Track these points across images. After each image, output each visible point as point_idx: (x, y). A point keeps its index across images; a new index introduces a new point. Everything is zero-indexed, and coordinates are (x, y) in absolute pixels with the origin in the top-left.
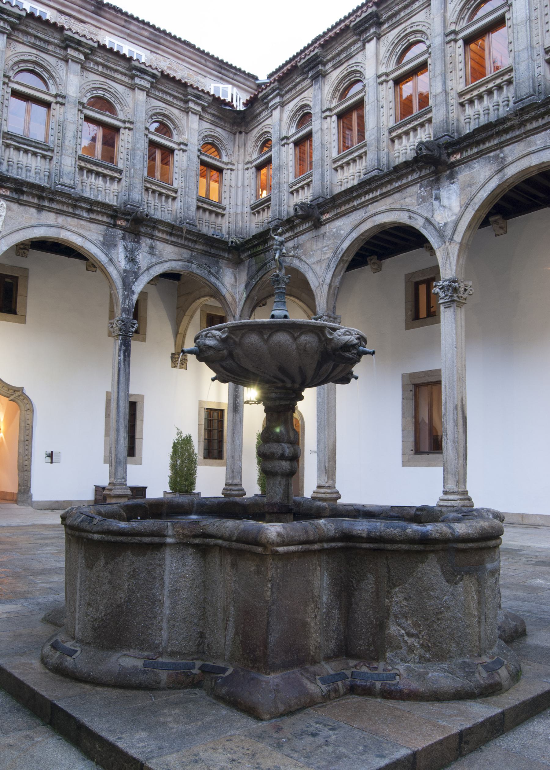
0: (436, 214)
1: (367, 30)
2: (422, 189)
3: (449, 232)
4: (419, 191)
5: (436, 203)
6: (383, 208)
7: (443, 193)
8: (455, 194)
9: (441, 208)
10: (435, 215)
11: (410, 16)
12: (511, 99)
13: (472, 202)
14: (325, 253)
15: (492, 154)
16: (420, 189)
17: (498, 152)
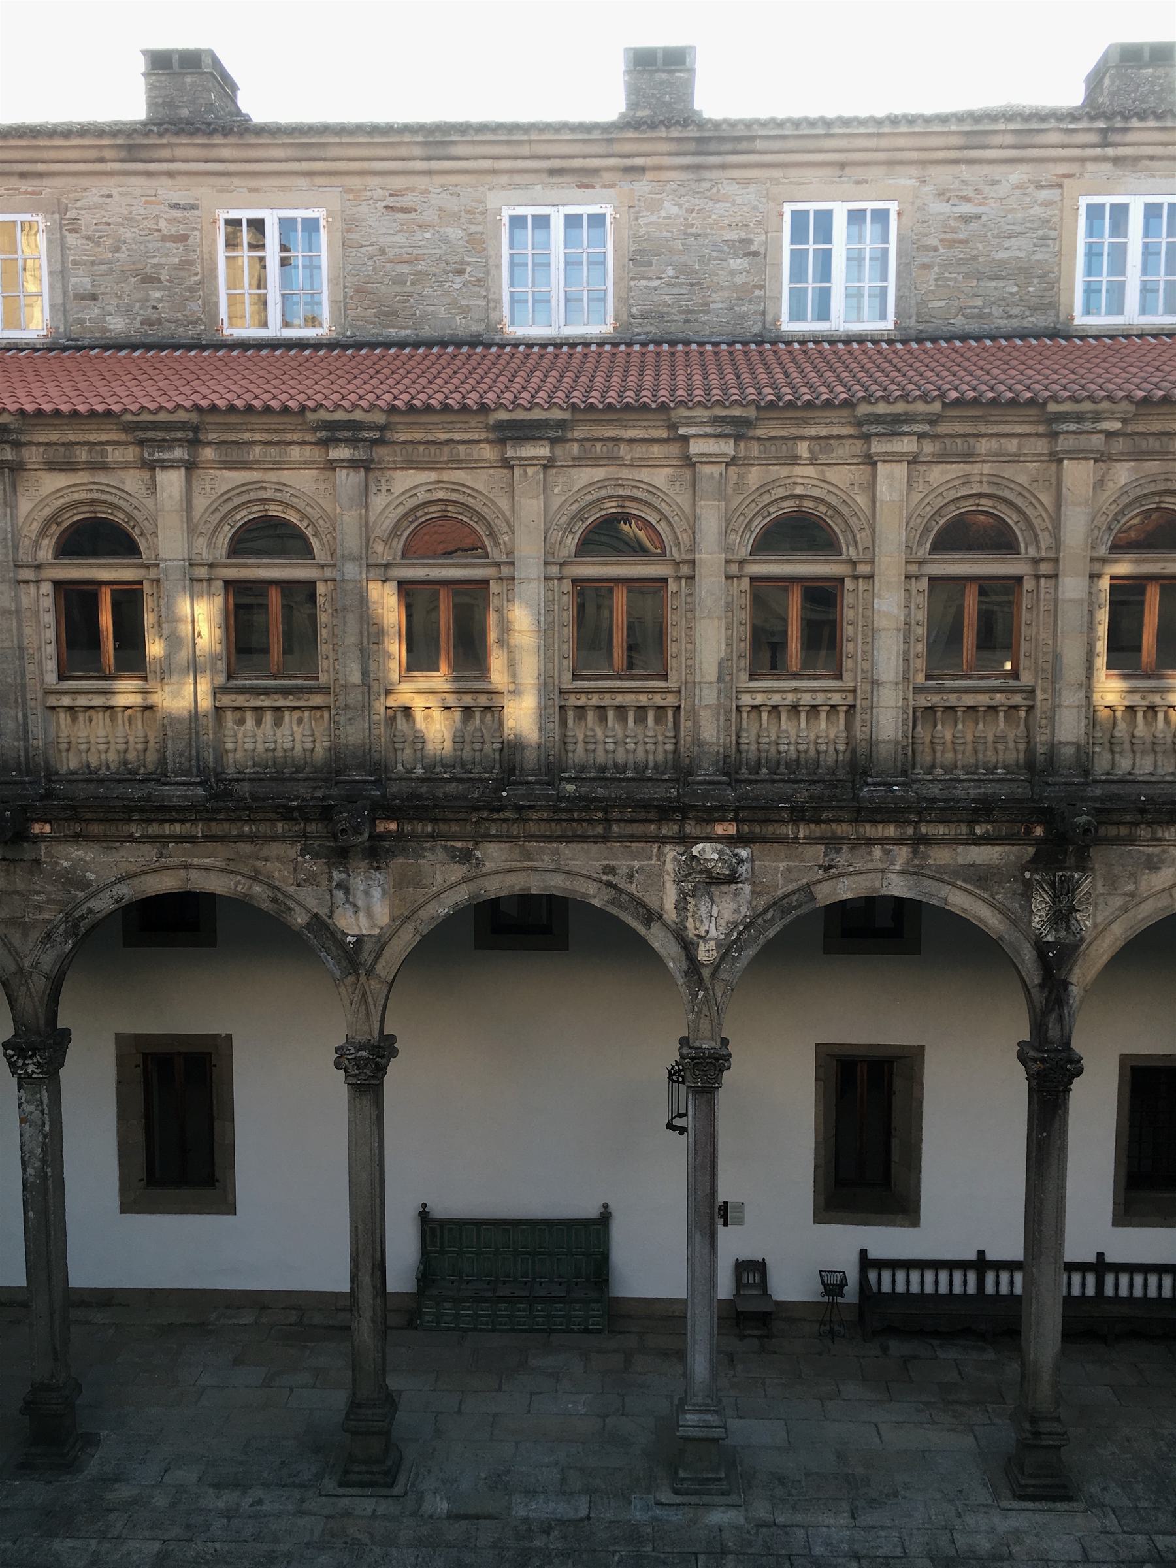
0: (338, 913)
1: (168, 444)
2: (307, 857)
3: (366, 956)
4: (300, 859)
5: (340, 894)
6: (207, 861)
7: (358, 884)
8: (379, 889)
9: (347, 906)
10: (335, 915)
11: (278, 465)
12: (487, 737)
13: (416, 916)
14: (39, 908)
15: (459, 845)
16: (303, 856)
17: (470, 845)
